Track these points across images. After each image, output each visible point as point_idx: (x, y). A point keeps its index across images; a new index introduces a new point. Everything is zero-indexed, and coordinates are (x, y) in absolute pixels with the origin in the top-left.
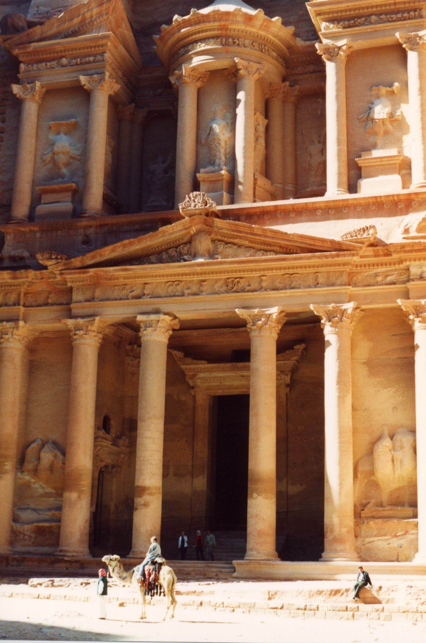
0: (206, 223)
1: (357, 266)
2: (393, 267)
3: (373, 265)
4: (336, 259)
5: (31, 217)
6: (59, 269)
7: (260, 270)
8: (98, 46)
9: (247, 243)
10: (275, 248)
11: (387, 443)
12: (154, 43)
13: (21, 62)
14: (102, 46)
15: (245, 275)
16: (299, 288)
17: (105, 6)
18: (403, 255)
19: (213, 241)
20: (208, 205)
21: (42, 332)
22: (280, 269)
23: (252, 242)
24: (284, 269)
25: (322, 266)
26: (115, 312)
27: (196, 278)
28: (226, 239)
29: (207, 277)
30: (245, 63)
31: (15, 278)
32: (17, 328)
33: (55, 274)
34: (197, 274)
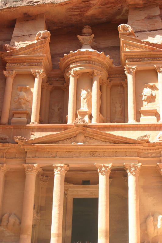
1: (141, 150)
2: (155, 151)
3: (147, 150)
4: (134, 146)
5: (9, 123)
6: (23, 144)
7: (104, 149)
8: (40, 59)
9: (99, 138)
10: (110, 141)
11: (152, 218)
12: (60, 61)
13: (7, 63)
14: (41, 59)
16: (119, 157)
17: (43, 45)
19: (85, 137)
20: (85, 123)
21: (11, 169)
23: (101, 138)
24: (114, 149)
25: (128, 149)
26: (45, 163)
27: (78, 151)
28: (90, 136)
29: (83, 151)
30: (97, 71)
31: (3, 146)
32: (3, 167)
33: (21, 146)
34: (79, 149)
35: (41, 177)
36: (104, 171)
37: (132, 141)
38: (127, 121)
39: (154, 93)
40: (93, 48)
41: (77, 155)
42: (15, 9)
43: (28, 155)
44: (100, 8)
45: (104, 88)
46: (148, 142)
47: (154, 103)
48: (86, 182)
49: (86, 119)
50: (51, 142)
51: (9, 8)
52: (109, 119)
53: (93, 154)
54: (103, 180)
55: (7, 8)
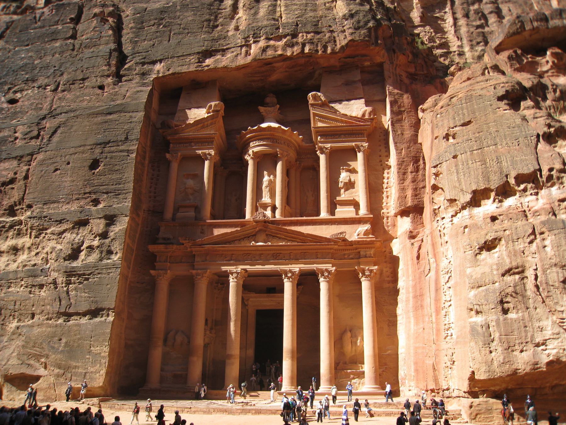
2: (352, 251)
5: (174, 219)
11: (349, 334)
14: (213, 138)
15: (283, 252)
19: (267, 235)
22: (300, 250)
27: (258, 253)
30: (281, 152)
31: (167, 249)
32: (166, 274)
34: (259, 250)
35: (216, 285)
36: (291, 277)
37: (324, 240)
39: (353, 177)
40: (278, 122)
41: (257, 258)
42: (180, 75)
43: (197, 259)
44: (286, 71)
45: (293, 173)
47: (353, 190)
50: (225, 243)
51: (173, 74)
52: (298, 211)
53: (277, 256)
55: (169, 74)
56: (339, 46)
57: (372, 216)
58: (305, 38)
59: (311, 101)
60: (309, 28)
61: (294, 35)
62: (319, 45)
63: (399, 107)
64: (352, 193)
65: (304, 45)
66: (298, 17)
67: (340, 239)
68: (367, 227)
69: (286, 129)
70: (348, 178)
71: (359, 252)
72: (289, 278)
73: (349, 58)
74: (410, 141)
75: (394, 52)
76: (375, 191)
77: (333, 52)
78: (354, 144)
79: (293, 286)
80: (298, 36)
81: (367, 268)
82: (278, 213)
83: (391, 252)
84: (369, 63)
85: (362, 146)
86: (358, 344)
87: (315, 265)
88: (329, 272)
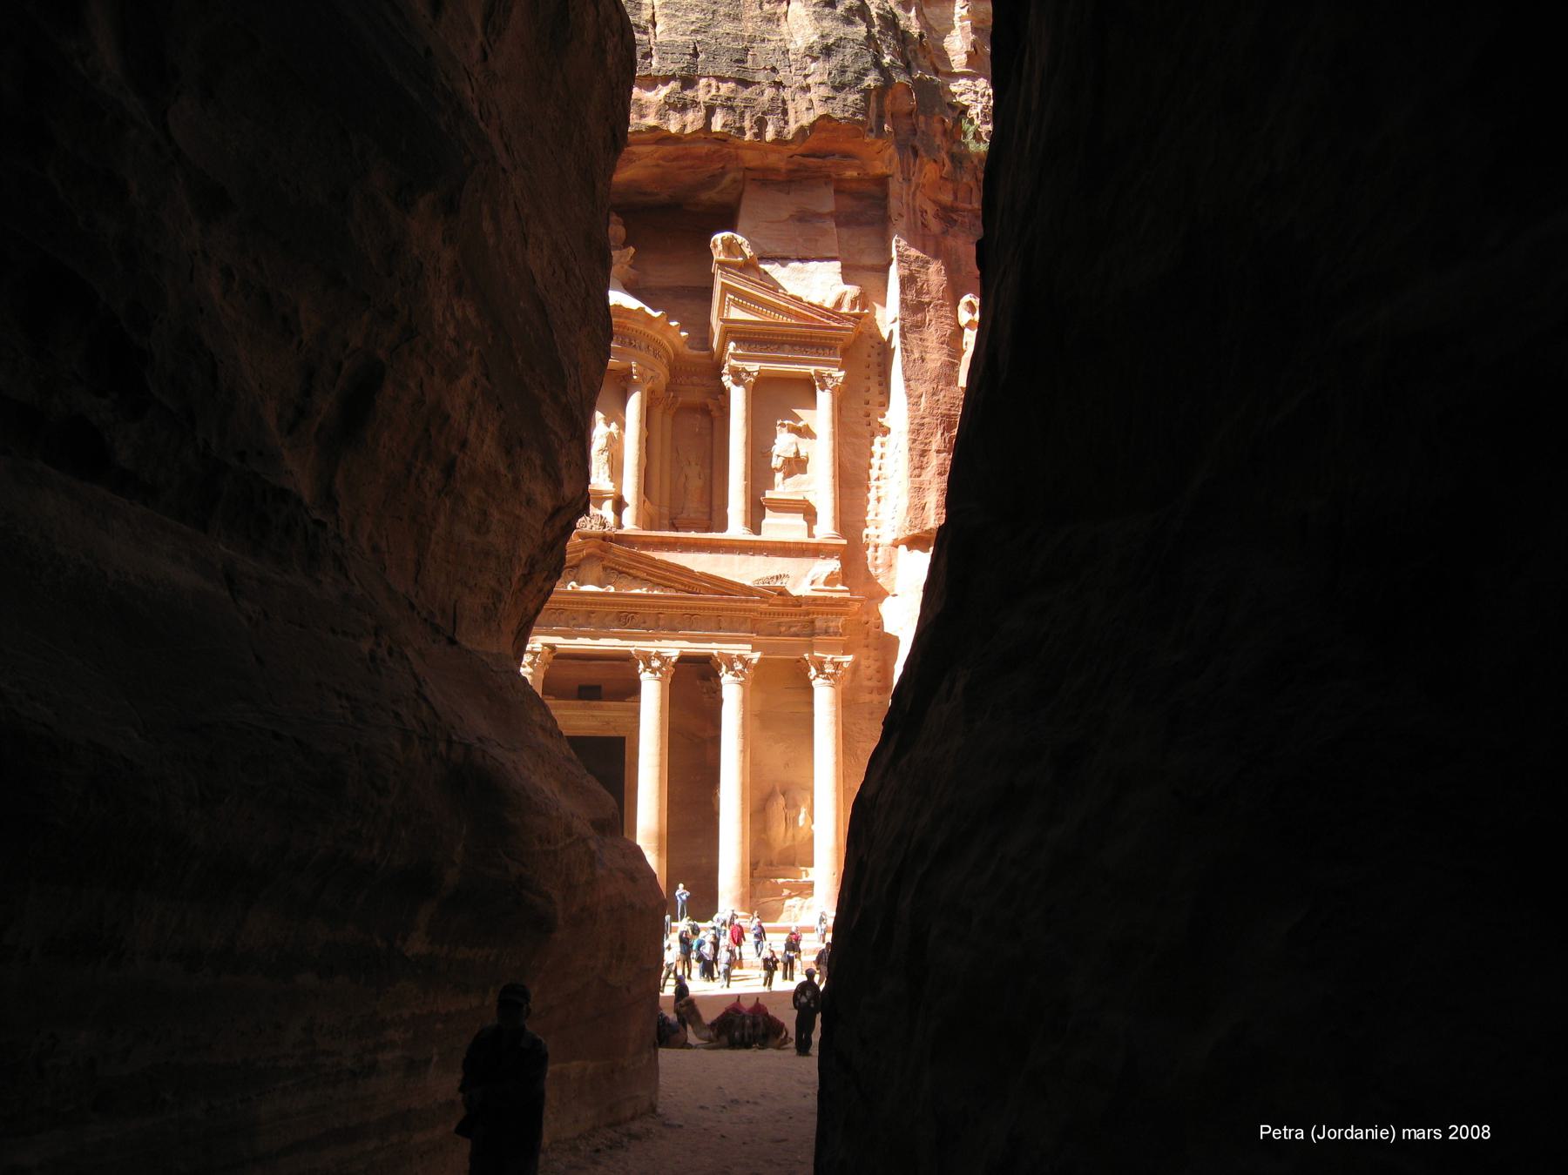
0: (600, 547)
11: (781, 801)
18: (812, 608)
19: (605, 568)
27: (585, 608)
36: (659, 669)
38: (723, 527)
39: (805, 447)
45: (657, 413)
46: (782, 593)
47: (804, 477)
48: (589, 693)
49: (607, 511)
53: (626, 617)
54: (651, 692)
56: (793, 127)
57: (844, 542)
58: (713, 92)
59: (719, 255)
60: (724, 67)
61: (689, 82)
62: (747, 116)
63: (919, 293)
64: (799, 484)
65: (710, 111)
66: (696, 32)
67: (774, 589)
68: (833, 565)
69: (656, 314)
70: (794, 449)
71: (812, 622)
72: (654, 671)
73: (814, 156)
74: (938, 378)
75: (916, 153)
76: (852, 481)
77: (779, 140)
78: (812, 369)
79: (662, 690)
80: (697, 83)
81: (829, 657)
82: (629, 516)
83: (880, 625)
84: (855, 174)
85: (830, 376)
86: (801, 823)
87: (714, 645)
88: (746, 663)
